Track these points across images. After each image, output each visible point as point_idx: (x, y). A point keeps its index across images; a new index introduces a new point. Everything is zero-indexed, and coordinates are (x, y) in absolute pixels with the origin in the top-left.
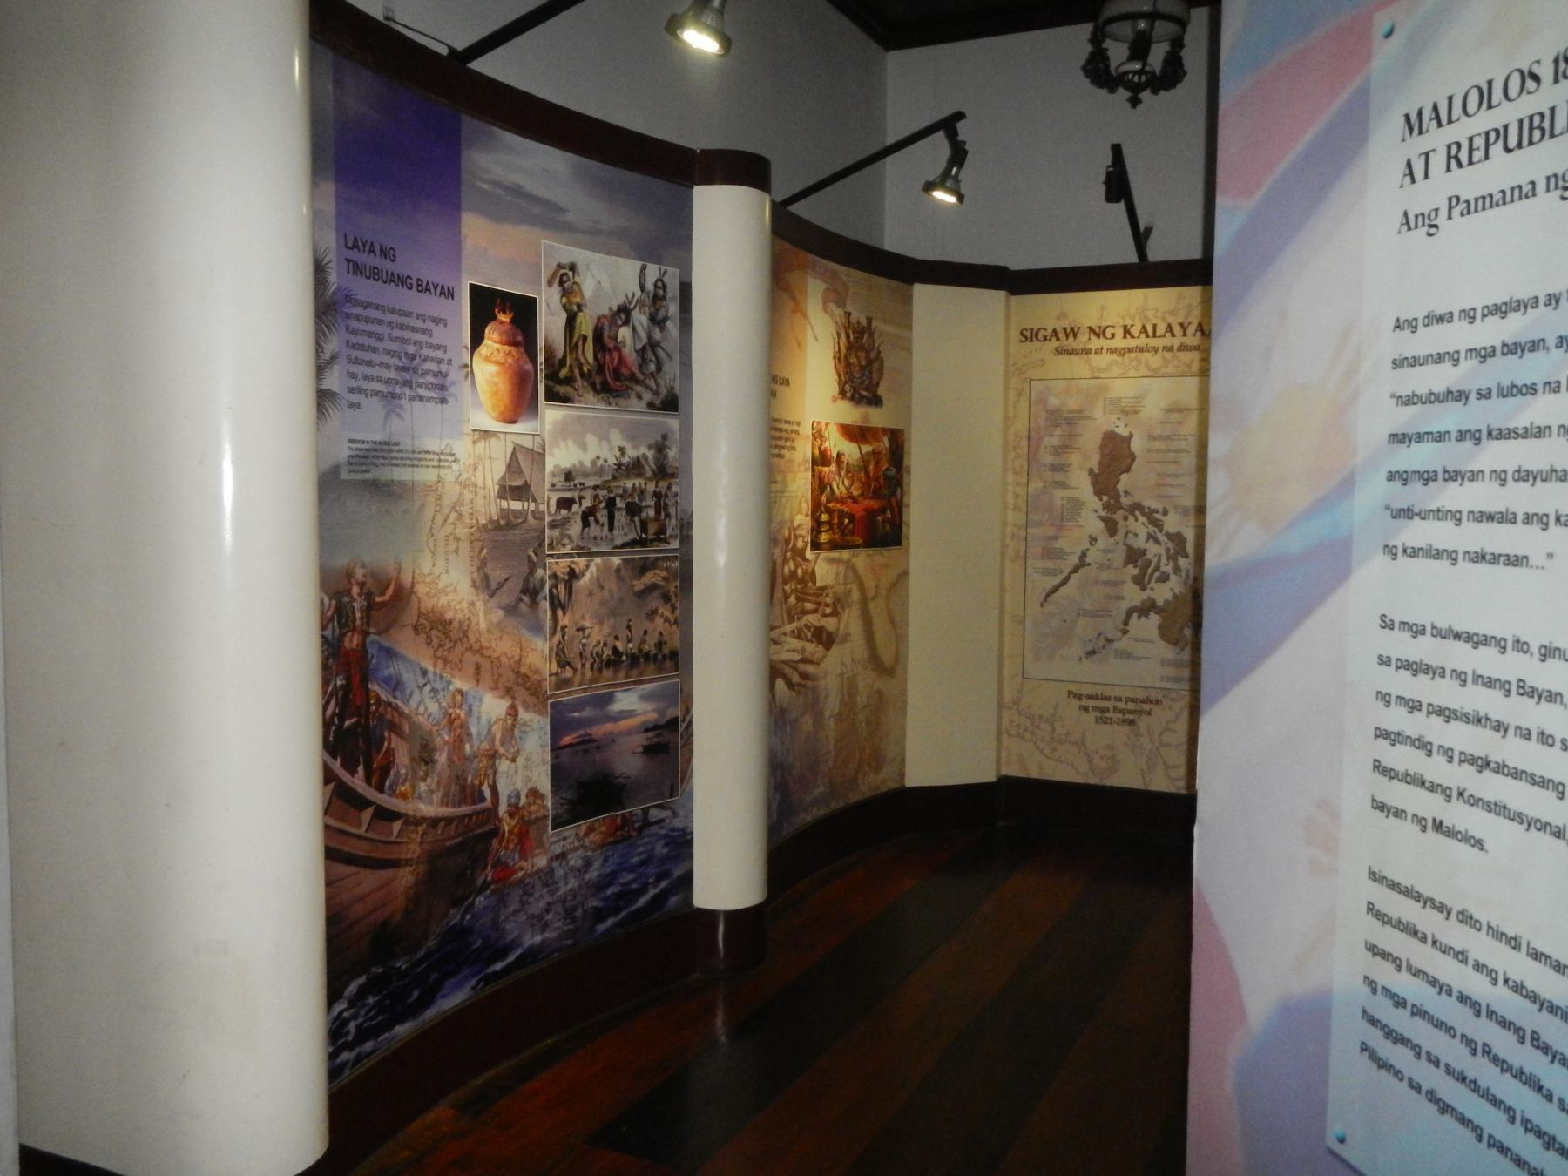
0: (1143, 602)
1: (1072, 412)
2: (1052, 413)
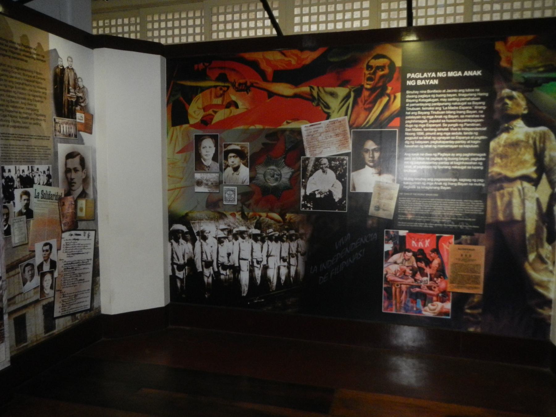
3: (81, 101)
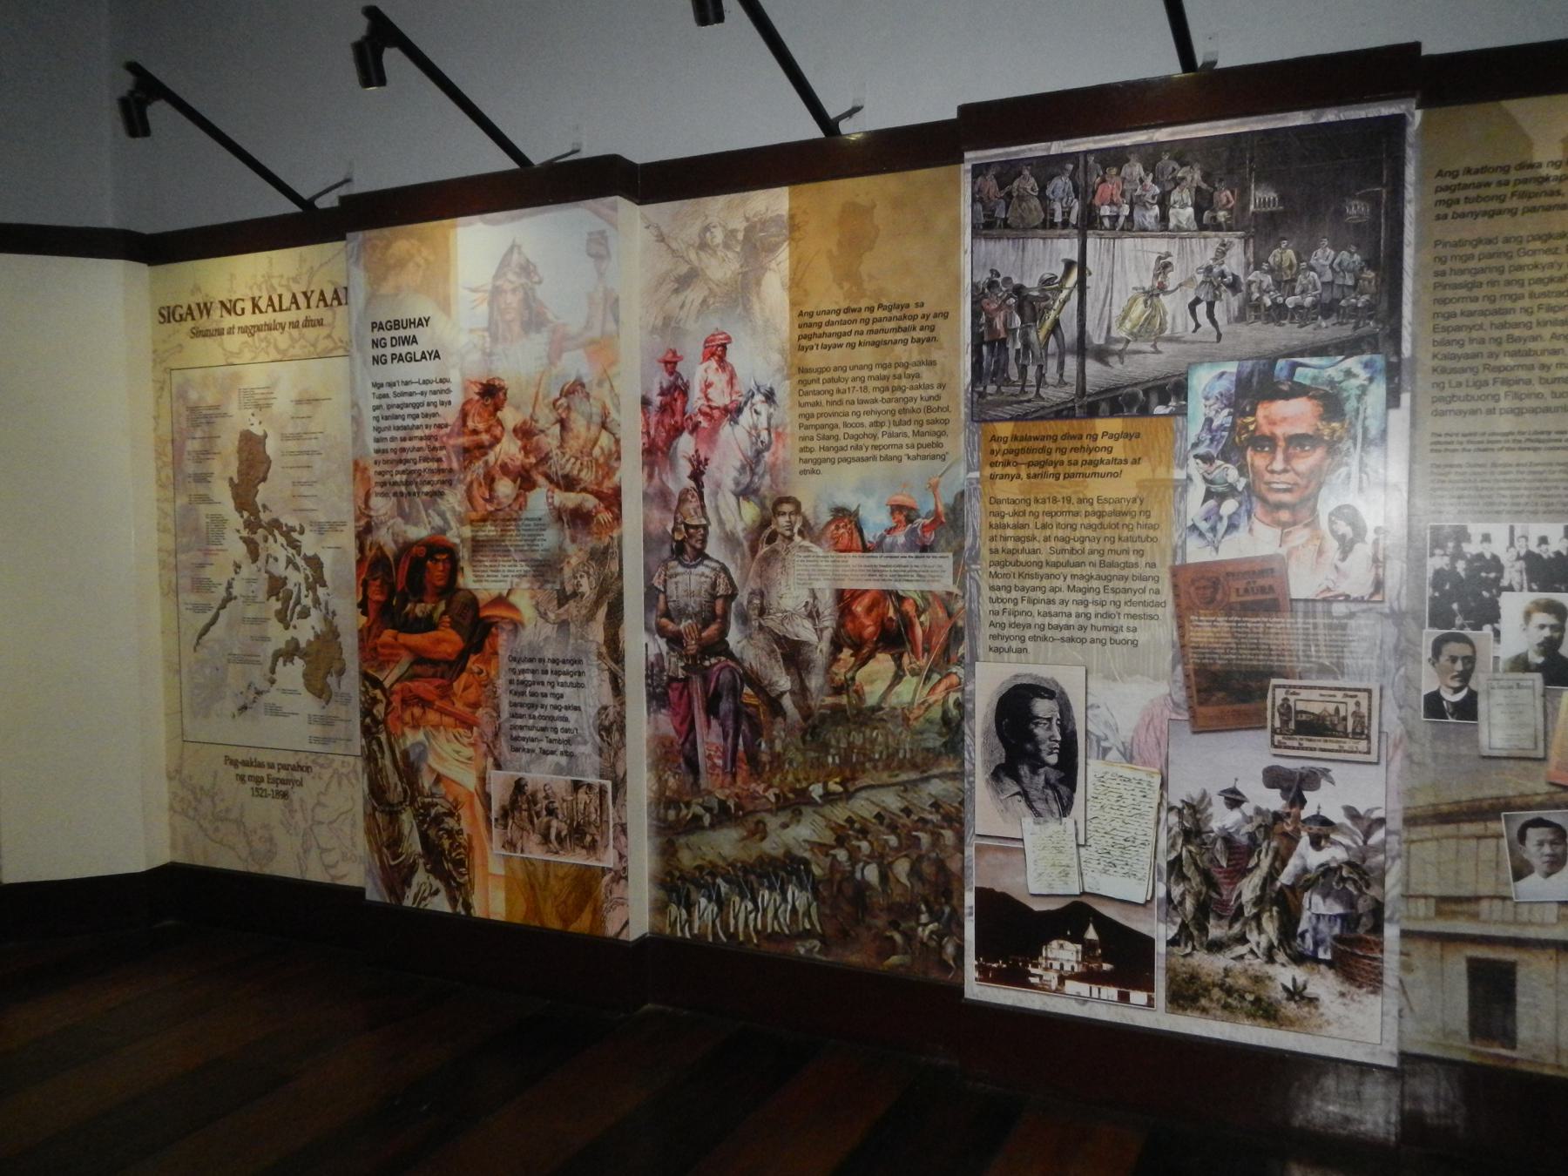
0: (288, 643)
1: (210, 408)
2: (193, 409)
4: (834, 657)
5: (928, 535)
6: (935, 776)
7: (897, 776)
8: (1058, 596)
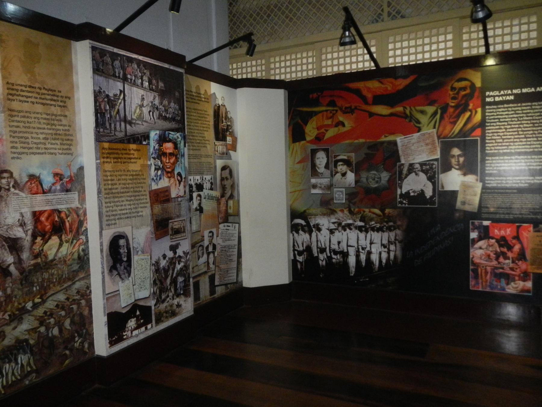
3: (229, 128)
4: (33, 242)
5: (68, 185)
6: (77, 281)
7: (63, 286)
8: (124, 203)
